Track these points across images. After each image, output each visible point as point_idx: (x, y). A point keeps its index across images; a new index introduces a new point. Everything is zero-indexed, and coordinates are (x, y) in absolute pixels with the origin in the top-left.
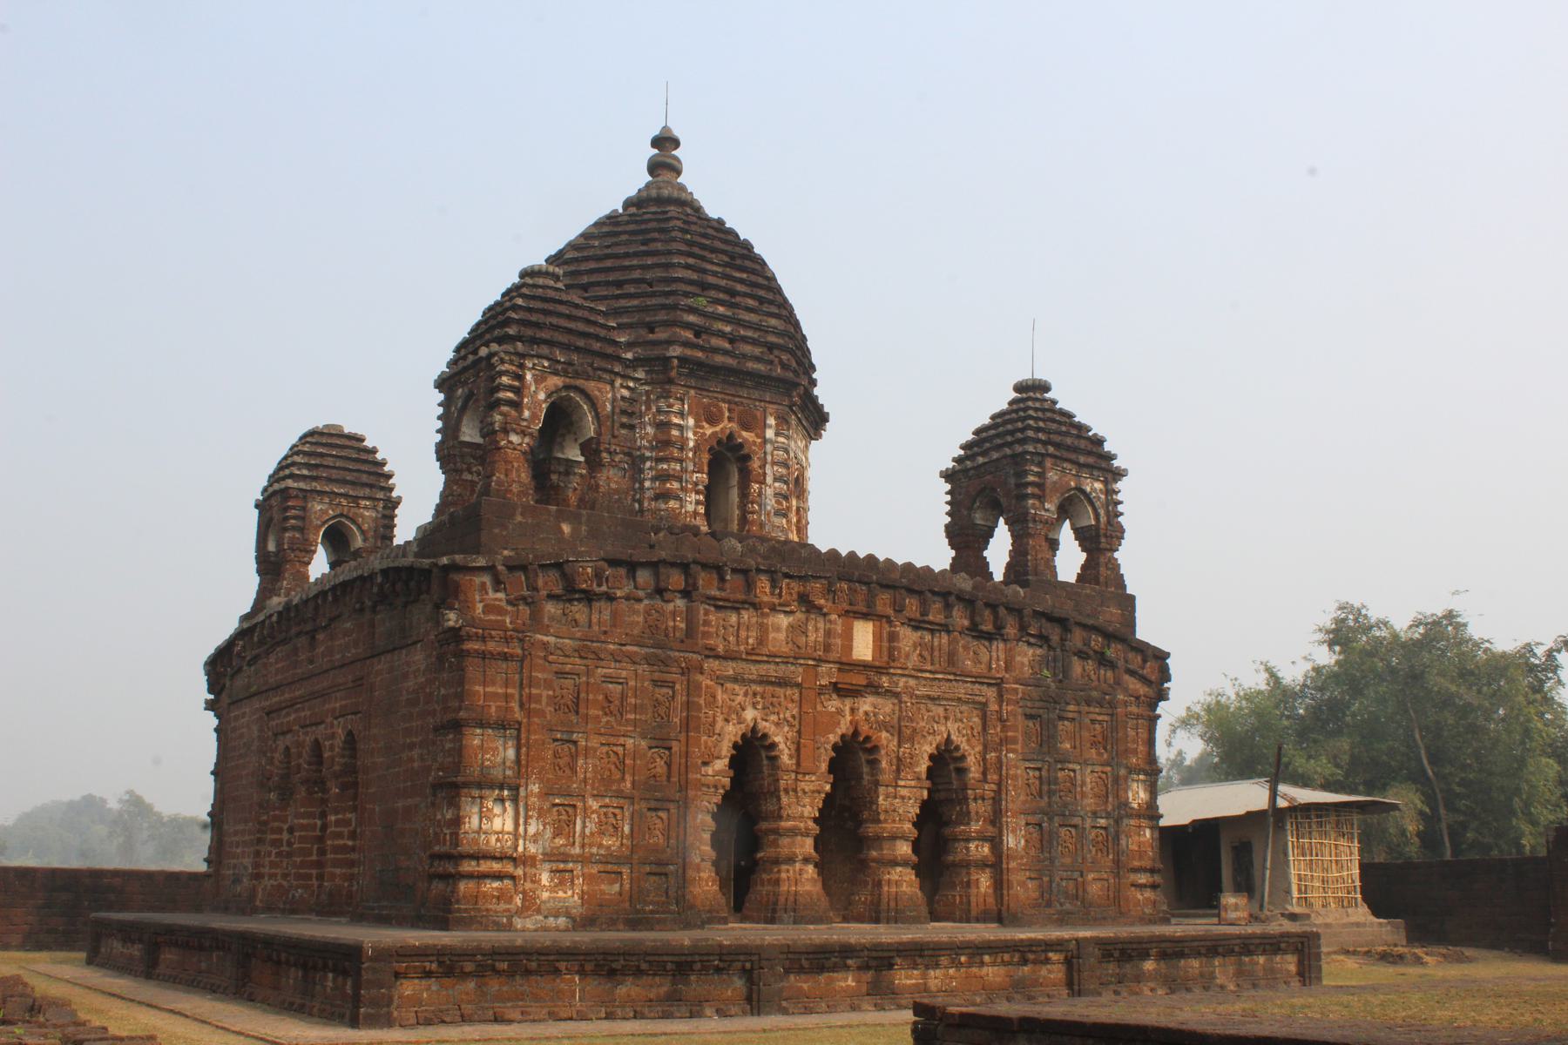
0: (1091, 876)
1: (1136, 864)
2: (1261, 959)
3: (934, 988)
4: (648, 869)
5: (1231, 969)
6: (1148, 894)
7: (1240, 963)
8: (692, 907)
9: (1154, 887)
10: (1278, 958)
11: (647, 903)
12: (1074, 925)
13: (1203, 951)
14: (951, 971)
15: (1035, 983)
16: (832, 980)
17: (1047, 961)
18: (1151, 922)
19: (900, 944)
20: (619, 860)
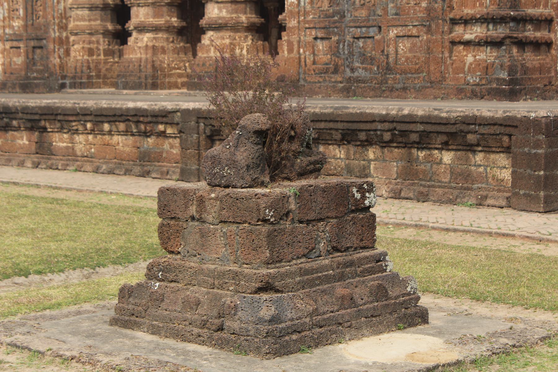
0: (393, 33)
1: (468, 11)
2: (447, 157)
3: (79, 153)
4: (32, 43)
5: (394, 167)
6: (486, 55)
7: (410, 160)
8: (51, 74)
9: (495, 44)
10: (479, 157)
11: (33, 72)
12: (363, 96)
13: (338, 136)
14: (90, 137)
15: (159, 157)
16: (14, 139)
17: (163, 134)
18: (476, 94)
19: (40, 108)
20: (16, 38)
